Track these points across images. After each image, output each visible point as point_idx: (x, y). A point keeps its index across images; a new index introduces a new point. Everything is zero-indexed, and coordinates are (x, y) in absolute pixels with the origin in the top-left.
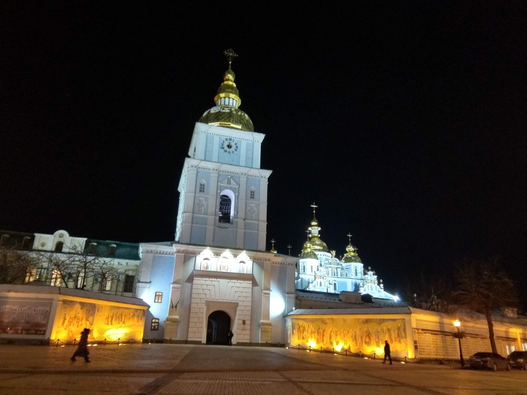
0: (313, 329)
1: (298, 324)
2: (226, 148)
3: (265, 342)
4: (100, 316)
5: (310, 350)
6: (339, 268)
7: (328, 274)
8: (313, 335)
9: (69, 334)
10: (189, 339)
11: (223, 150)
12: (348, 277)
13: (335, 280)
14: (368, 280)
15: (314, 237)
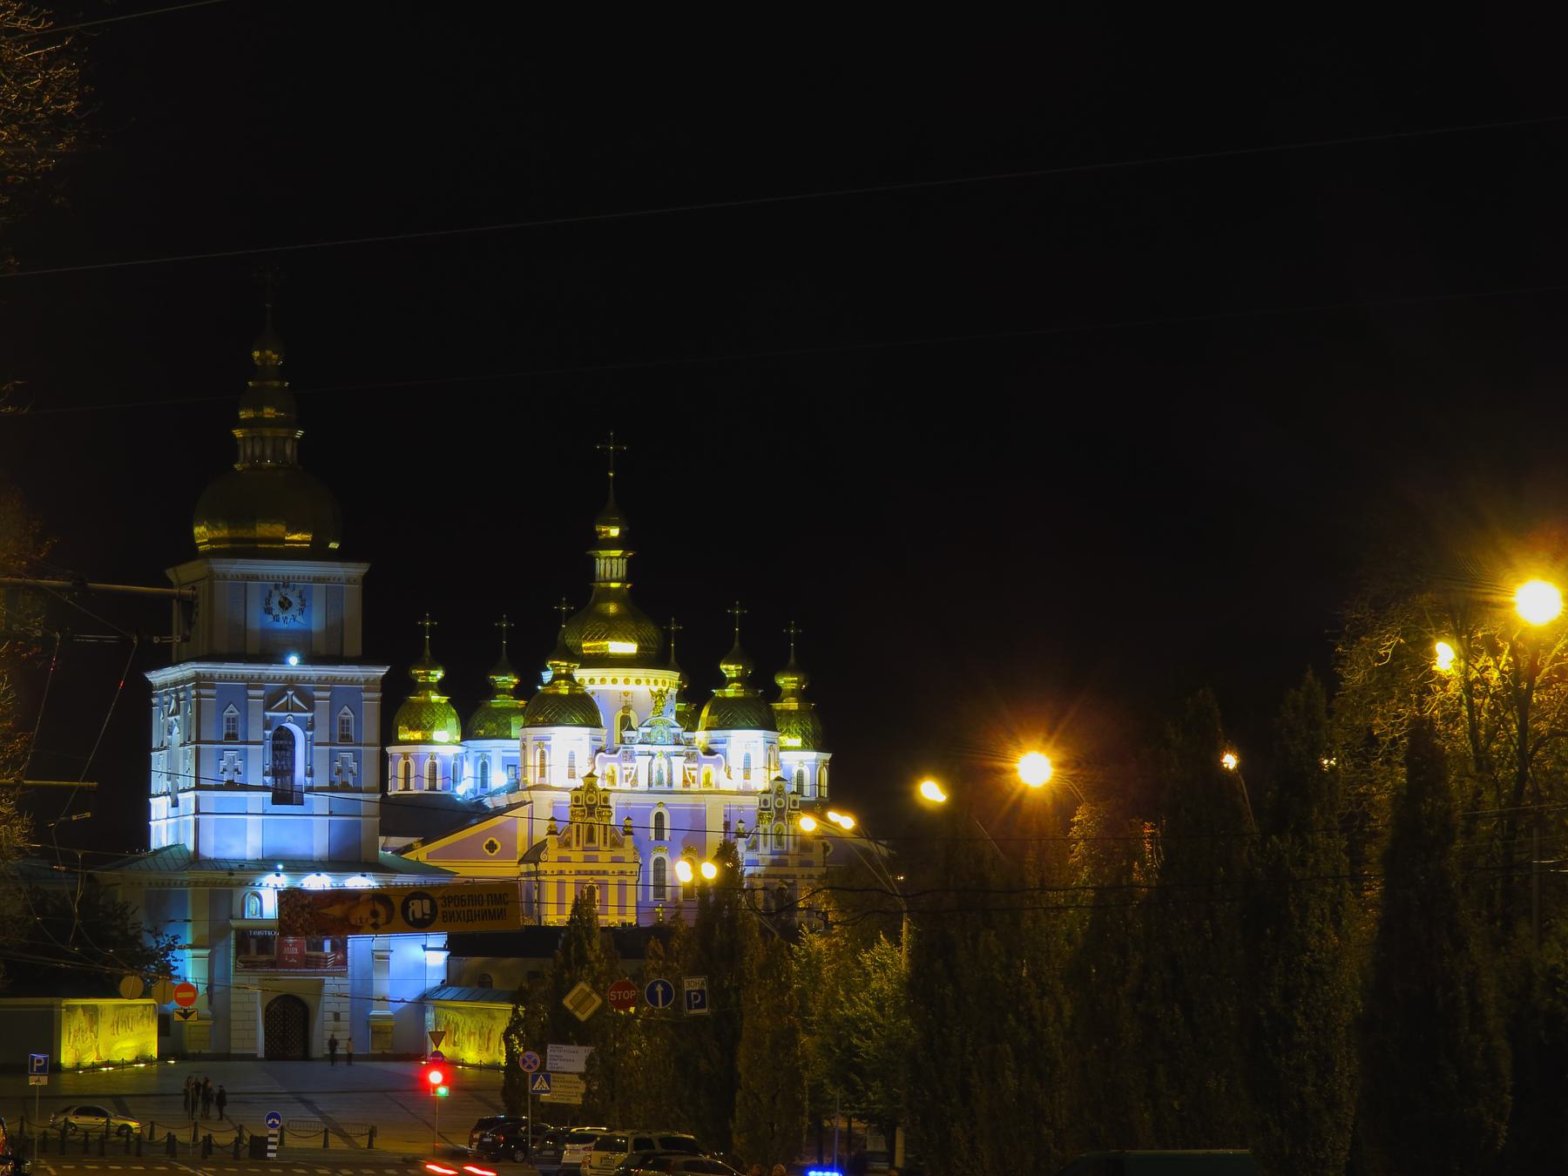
0: (472, 1026)
1: (446, 1018)
2: (277, 610)
3: (379, 1052)
4: (105, 1023)
5: (463, 1064)
6: (678, 755)
7: (634, 783)
8: (472, 1038)
9: (76, 1055)
10: (233, 1052)
11: (271, 616)
12: (713, 789)
13: (661, 804)
14: (768, 809)
15: (609, 595)
